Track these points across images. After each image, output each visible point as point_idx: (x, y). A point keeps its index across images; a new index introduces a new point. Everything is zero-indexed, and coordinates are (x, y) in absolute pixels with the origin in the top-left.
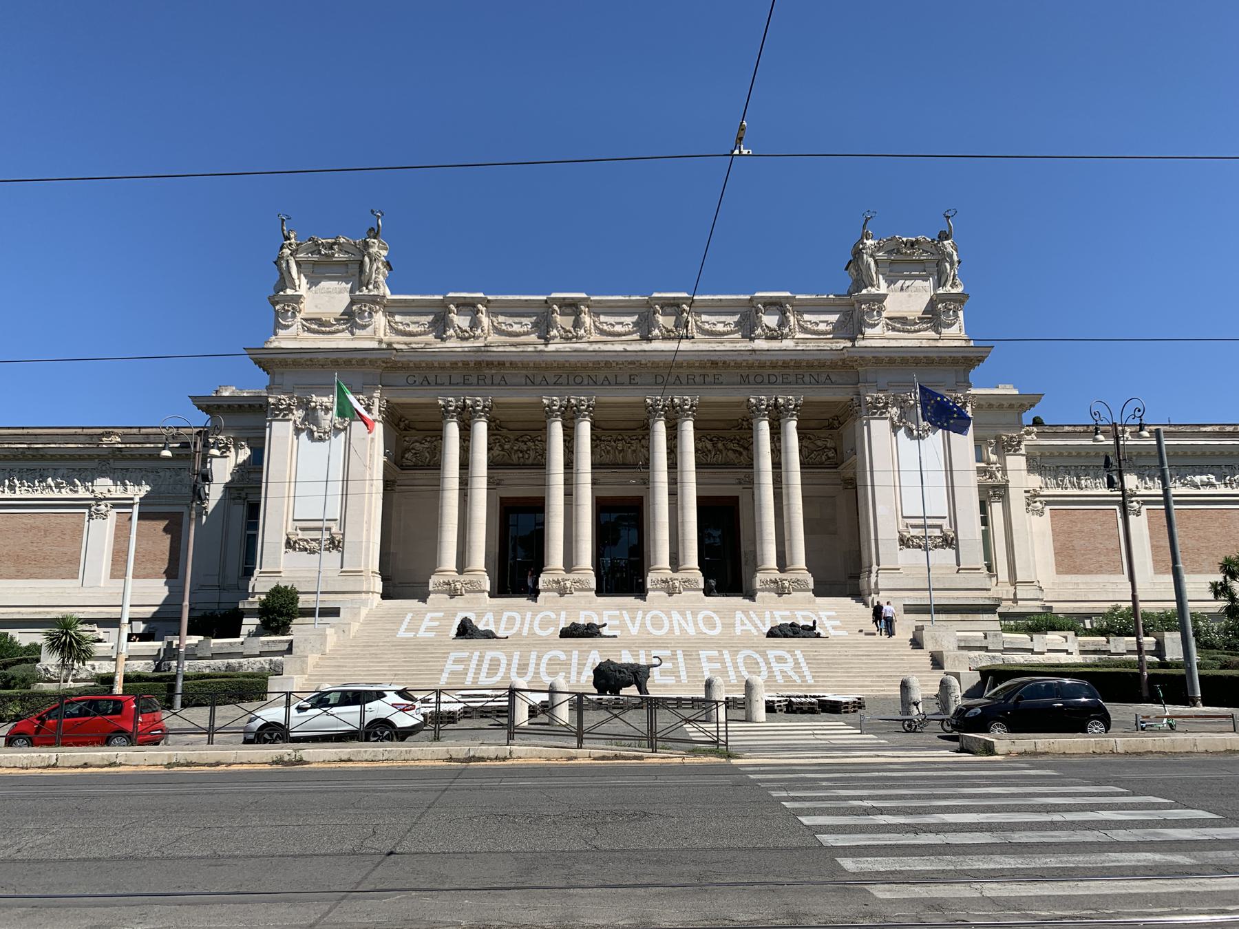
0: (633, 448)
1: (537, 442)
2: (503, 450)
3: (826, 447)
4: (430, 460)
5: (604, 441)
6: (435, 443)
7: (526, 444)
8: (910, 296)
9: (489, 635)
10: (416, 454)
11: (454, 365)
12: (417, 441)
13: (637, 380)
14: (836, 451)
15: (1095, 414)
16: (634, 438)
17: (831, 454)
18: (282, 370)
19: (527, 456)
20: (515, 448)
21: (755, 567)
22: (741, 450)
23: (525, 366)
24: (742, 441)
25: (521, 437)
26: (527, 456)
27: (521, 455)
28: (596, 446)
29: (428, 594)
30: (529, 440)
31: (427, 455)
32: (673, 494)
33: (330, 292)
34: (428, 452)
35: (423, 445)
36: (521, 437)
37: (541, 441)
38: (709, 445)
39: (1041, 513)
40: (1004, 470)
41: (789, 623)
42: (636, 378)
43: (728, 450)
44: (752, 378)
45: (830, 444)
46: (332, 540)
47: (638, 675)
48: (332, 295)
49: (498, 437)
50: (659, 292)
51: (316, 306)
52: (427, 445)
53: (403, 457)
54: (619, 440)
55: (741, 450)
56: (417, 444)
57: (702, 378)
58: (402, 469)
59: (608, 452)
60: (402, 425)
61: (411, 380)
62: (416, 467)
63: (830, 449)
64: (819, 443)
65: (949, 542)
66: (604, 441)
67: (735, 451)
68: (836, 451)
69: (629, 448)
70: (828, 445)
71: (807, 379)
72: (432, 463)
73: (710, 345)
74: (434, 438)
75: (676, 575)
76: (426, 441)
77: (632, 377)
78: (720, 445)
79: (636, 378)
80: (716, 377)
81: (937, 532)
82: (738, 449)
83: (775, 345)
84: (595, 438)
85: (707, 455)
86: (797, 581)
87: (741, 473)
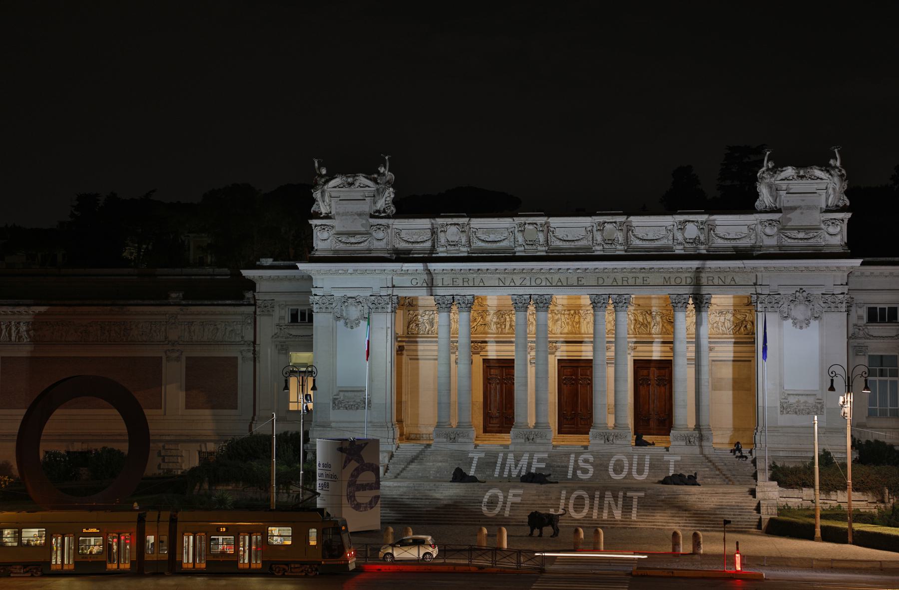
6: (433, 315)
8: (802, 213)
9: (473, 479)
13: (584, 282)
15: (832, 373)
18: (322, 277)
34: (428, 324)
35: (423, 318)
41: (679, 474)
42: (583, 280)
44: (672, 280)
47: (551, 520)
51: (344, 226)
53: (408, 327)
57: (634, 279)
61: (414, 282)
72: (430, 332)
74: (431, 313)
76: (425, 313)
77: (580, 279)
79: (583, 280)
80: (645, 279)
85: (647, 326)
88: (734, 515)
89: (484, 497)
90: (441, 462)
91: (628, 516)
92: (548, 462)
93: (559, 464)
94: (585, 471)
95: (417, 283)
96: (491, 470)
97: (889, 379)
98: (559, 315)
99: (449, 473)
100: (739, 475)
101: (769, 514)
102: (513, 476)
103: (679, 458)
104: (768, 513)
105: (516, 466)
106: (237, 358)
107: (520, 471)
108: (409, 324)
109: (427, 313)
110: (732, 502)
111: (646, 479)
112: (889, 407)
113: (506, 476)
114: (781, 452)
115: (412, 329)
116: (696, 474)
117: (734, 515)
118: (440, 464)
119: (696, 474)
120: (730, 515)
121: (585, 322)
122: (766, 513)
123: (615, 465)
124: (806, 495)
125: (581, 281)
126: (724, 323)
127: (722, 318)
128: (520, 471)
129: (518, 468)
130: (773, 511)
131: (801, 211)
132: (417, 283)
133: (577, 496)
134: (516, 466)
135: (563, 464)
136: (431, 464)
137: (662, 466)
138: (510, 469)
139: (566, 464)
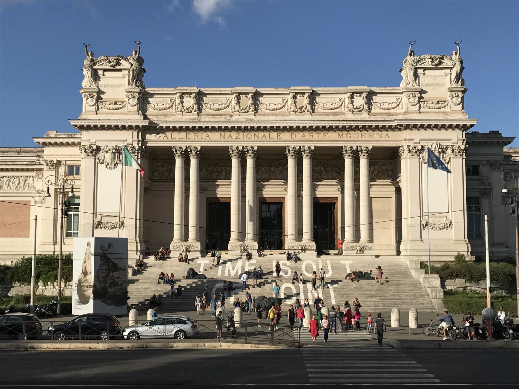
0: (280, 170)
1: (226, 167)
2: (208, 171)
3: (387, 170)
4: (167, 177)
5: (263, 166)
6: (170, 167)
7: (220, 168)
8: (434, 89)
10: (159, 173)
12: (160, 166)
14: (393, 172)
16: (281, 164)
19: (221, 174)
20: (214, 170)
22: (340, 171)
24: (341, 166)
25: (218, 163)
26: (221, 174)
27: (217, 174)
28: (259, 169)
30: (222, 165)
31: (166, 174)
33: (112, 87)
34: (167, 172)
35: (164, 168)
36: (218, 163)
37: (228, 166)
38: (323, 169)
43: (333, 171)
48: (114, 88)
49: (205, 164)
50: (295, 86)
52: (166, 168)
53: (153, 175)
54: (272, 166)
55: (340, 171)
56: (161, 168)
58: (153, 182)
59: (266, 172)
60: (152, 156)
62: (160, 180)
64: (384, 167)
66: (263, 166)
67: (336, 172)
68: (393, 172)
69: (277, 170)
70: (389, 169)
72: (168, 178)
73: (322, 117)
74: (170, 164)
78: (328, 169)
81: (444, 220)
82: (338, 170)
83: (358, 117)
84: (258, 164)
85: (321, 174)
88: (410, 299)
89: (212, 289)
90: (176, 266)
91: (329, 302)
92: (256, 265)
93: (265, 267)
94: (286, 273)
95: (160, 137)
96: (215, 272)
97: (474, 213)
98: (260, 166)
99: (183, 274)
100: (398, 273)
101: (438, 298)
102: (232, 275)
103: (352, 262)
104: (437, 297)
105: (233, 269)
106: (30, 201)
107: (237, 272)
108: (153, 172)
109: (166, 165)
110: (406, 290)
111: (331, 276)
112: (475, 232)
113: (227, 275)
114: (424, 257)
115: (155, 176)
116: (371, 271)
117: (410, 299)
118: (176, 268)
119: (371, 271)
120: (408, 299)
121: (278, 171)
122: (435, 297)
123: (306, 267)
124: (460, 284)
125: (279, 136)
126: (373, 172)
127: (372, 168)
128: (237, 272)
129: (235, 270)
130: (440, 296)
131: (433, 87)
132: (160, 137)
133: (286, 287)
134: (233, 269)
135: (268, 267)
136: (169, 268)
137: (341, 267)
138: (229, 269)
139: (270, 267)
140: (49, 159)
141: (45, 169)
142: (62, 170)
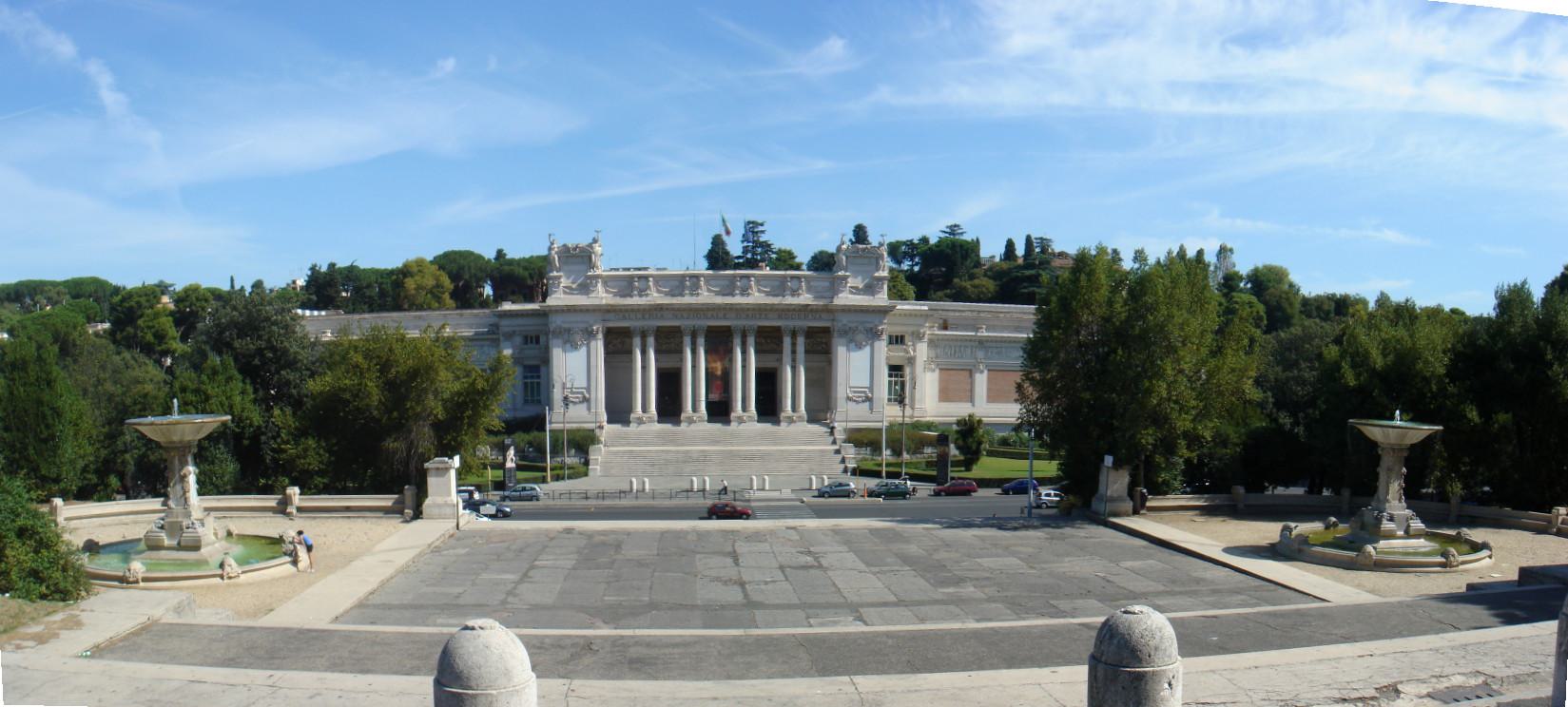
11: (638, 310)
17: (824, 346)
21: (781, 410)
23: (673, 309)
29: (630, 422)
32: (744, 367)
39: (934, 371)
40: (914, 351)
45: (824, 340)
46: (584, 397)
52: (619, 340)
63: (822, 343)
64: (819, 340)
65: (869, 400)
71: (810, 316)
75: (745, 414)
86: (800, 417)
87: (777, 356)
140: (506, 329)
141: (502, 338)
142: (518, 340)
